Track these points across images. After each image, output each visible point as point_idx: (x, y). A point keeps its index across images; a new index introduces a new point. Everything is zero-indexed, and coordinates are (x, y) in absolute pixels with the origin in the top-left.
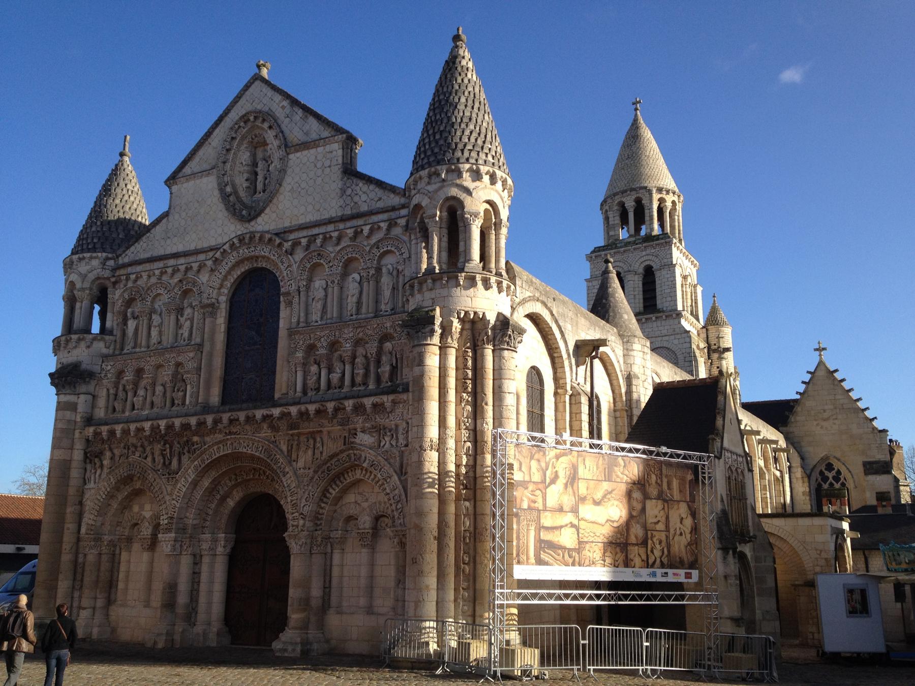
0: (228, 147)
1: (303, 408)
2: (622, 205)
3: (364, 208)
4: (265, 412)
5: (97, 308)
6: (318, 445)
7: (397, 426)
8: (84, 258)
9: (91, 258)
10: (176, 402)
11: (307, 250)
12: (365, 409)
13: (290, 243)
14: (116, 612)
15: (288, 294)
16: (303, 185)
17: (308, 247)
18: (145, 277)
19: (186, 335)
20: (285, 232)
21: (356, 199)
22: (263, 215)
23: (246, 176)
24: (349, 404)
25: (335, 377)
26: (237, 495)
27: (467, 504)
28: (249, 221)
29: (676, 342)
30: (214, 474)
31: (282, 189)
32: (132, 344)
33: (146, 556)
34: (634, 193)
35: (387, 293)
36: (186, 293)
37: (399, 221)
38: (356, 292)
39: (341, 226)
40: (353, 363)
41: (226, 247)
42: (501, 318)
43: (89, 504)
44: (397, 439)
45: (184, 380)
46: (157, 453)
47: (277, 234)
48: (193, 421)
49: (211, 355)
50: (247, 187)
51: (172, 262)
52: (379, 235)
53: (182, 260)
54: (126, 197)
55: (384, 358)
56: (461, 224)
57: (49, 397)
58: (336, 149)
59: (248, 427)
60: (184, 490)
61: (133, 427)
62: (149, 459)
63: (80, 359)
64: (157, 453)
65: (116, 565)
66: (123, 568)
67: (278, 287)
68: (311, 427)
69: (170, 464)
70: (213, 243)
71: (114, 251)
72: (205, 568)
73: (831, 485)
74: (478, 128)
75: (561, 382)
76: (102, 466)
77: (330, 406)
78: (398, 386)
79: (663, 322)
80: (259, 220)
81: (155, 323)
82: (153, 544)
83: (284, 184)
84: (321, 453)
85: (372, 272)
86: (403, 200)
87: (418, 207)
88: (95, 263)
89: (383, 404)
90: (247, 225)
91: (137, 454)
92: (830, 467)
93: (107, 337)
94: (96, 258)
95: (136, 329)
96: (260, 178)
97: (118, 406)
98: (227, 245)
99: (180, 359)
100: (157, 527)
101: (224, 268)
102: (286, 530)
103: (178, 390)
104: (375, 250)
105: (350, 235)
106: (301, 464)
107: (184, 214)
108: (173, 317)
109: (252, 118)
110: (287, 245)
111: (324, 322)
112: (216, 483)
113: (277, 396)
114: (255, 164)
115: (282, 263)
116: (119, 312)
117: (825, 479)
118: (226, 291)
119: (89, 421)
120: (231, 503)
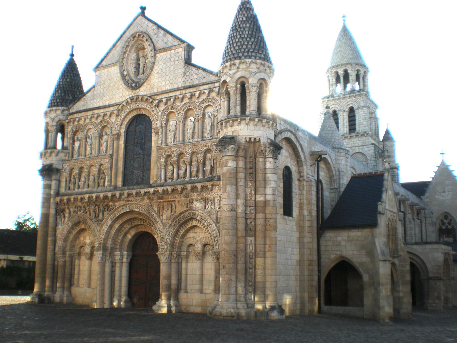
0: (125, 51)
1: (165, 188)
2: (337, 73)
3: (196, 82)
4: (146, 190)
5: (59, 135)
6: (174, 208)
7: (214, 198)
8: (53, 110)
9: (56, 110)
10: (100, 184)
11: (166, 105)
12: (198, 189)
13: (157, 101)
14: (75, 290)
15: (157, 128)
16: (164, 70)
17: (166, 103)
18: (83, 119)
19: (104, 149)
20: (154, 95)
21: (192, 77)
22: (143, 86)
23: (134, 66)
24: (189, 187)
25: (182, 172)
26: (133, 232)
27: (251, 238)
28: (136, 90)
29: (366, 149)
30: (120, 222)
31: (153, 73)
32: (77, 155)
33: (87, 262)
34: (343, 66)
35: (208, 127)
36: (104, 127)
37: (214, 89)
38: (192, 127)
39: (184, 92)
40: (191, 165)
41: (124, 103)
42: (269, 141)
43: (59, 235)
44: (214, 205)
45: (104, 173)
46: (92, 211)
47: (150, 97)
48: (109, 194)
49: (117, 160)
50: (135, 72)
51: (96, 112)
52: (204, 97)
53: (102, 111)
54: (73, 78)
55: (207, 163)
56: (247, 91)
57: (39, 182)
58: (181, 51)
59: (137, 198)
60: (106, 229)
61: (79, 197)
62: (88, 214)
63: (52, 162)
64: (92, 211)
65: (73, 266)
66: (76, 268)
67: (151, 125)
68: (170, 198)
69: (98, 216)
70: (117, 101)
71: (67, 106)
72: (117, 269)
74: (256, 40)
75: (301, 174)
76: (64, 217)
77: (179, 188)
78: (215, 177)
79: (360, 139)
80: (141, 89)
81: (89, 144)
82: (91, 257)
83: (154, 70)
84: (175, 212)
85: (200, 116)
86: (217, 78)
87: (225, 82)
88: (59, 112)
89: (207, 186)
90: (135, 91)
91: (82, 211)
93: (65, 151)
94: (59, 109)
95: (79, 147)
96: (141, 67)
97: (72, 186)
98: (125, 102)
99: (102, 162)
100: (93, 247)
101: (123, 115)
102: (157, 251)
103: (101, 179)
104: (202, 105)
105: (189, 97)
106: (164, 217)
107: (102, 86)
108: (97, 140)
109: (137, 35)
110: (156, 102)
111: (175, 143)
112: (122, 226)
113: (151, 182)
114: (138, 59)
115: (153, 111)
116: (70, 138)
118: (124, 127)
119: (58, 194)
120: (129, 237)
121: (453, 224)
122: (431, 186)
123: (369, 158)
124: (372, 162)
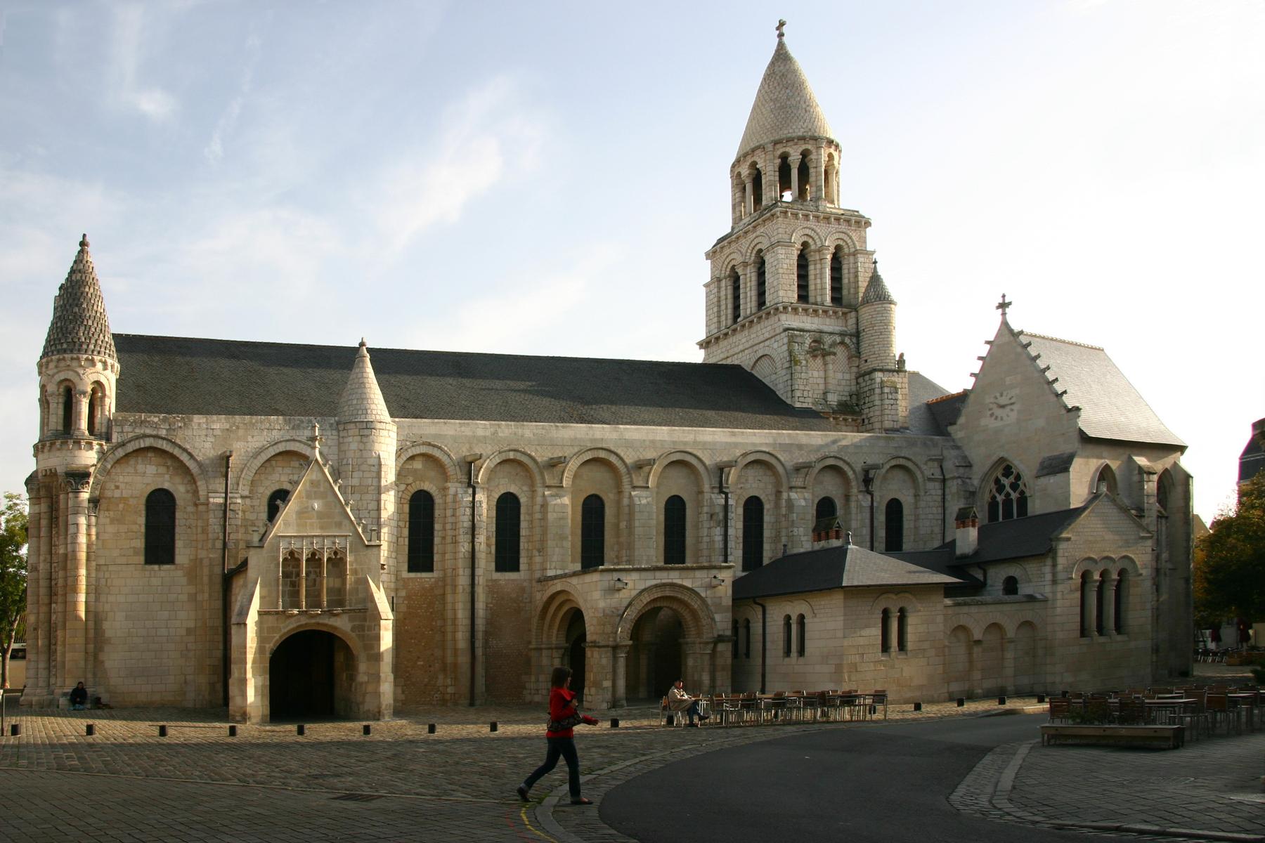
29: (775, 346)
73: (1008, 494)
92: (1008, 471)
117: (1000, 488)
121: (1022, 487)
122: (972, 397)
123: (779, 365)
124: (784, 372)
